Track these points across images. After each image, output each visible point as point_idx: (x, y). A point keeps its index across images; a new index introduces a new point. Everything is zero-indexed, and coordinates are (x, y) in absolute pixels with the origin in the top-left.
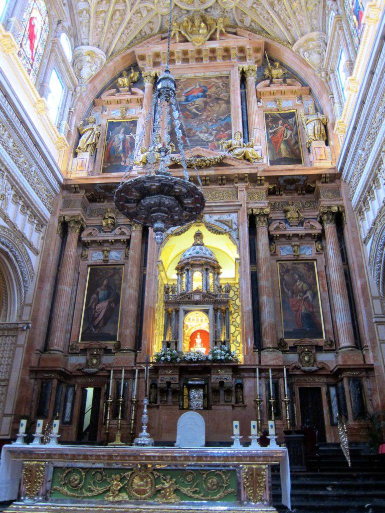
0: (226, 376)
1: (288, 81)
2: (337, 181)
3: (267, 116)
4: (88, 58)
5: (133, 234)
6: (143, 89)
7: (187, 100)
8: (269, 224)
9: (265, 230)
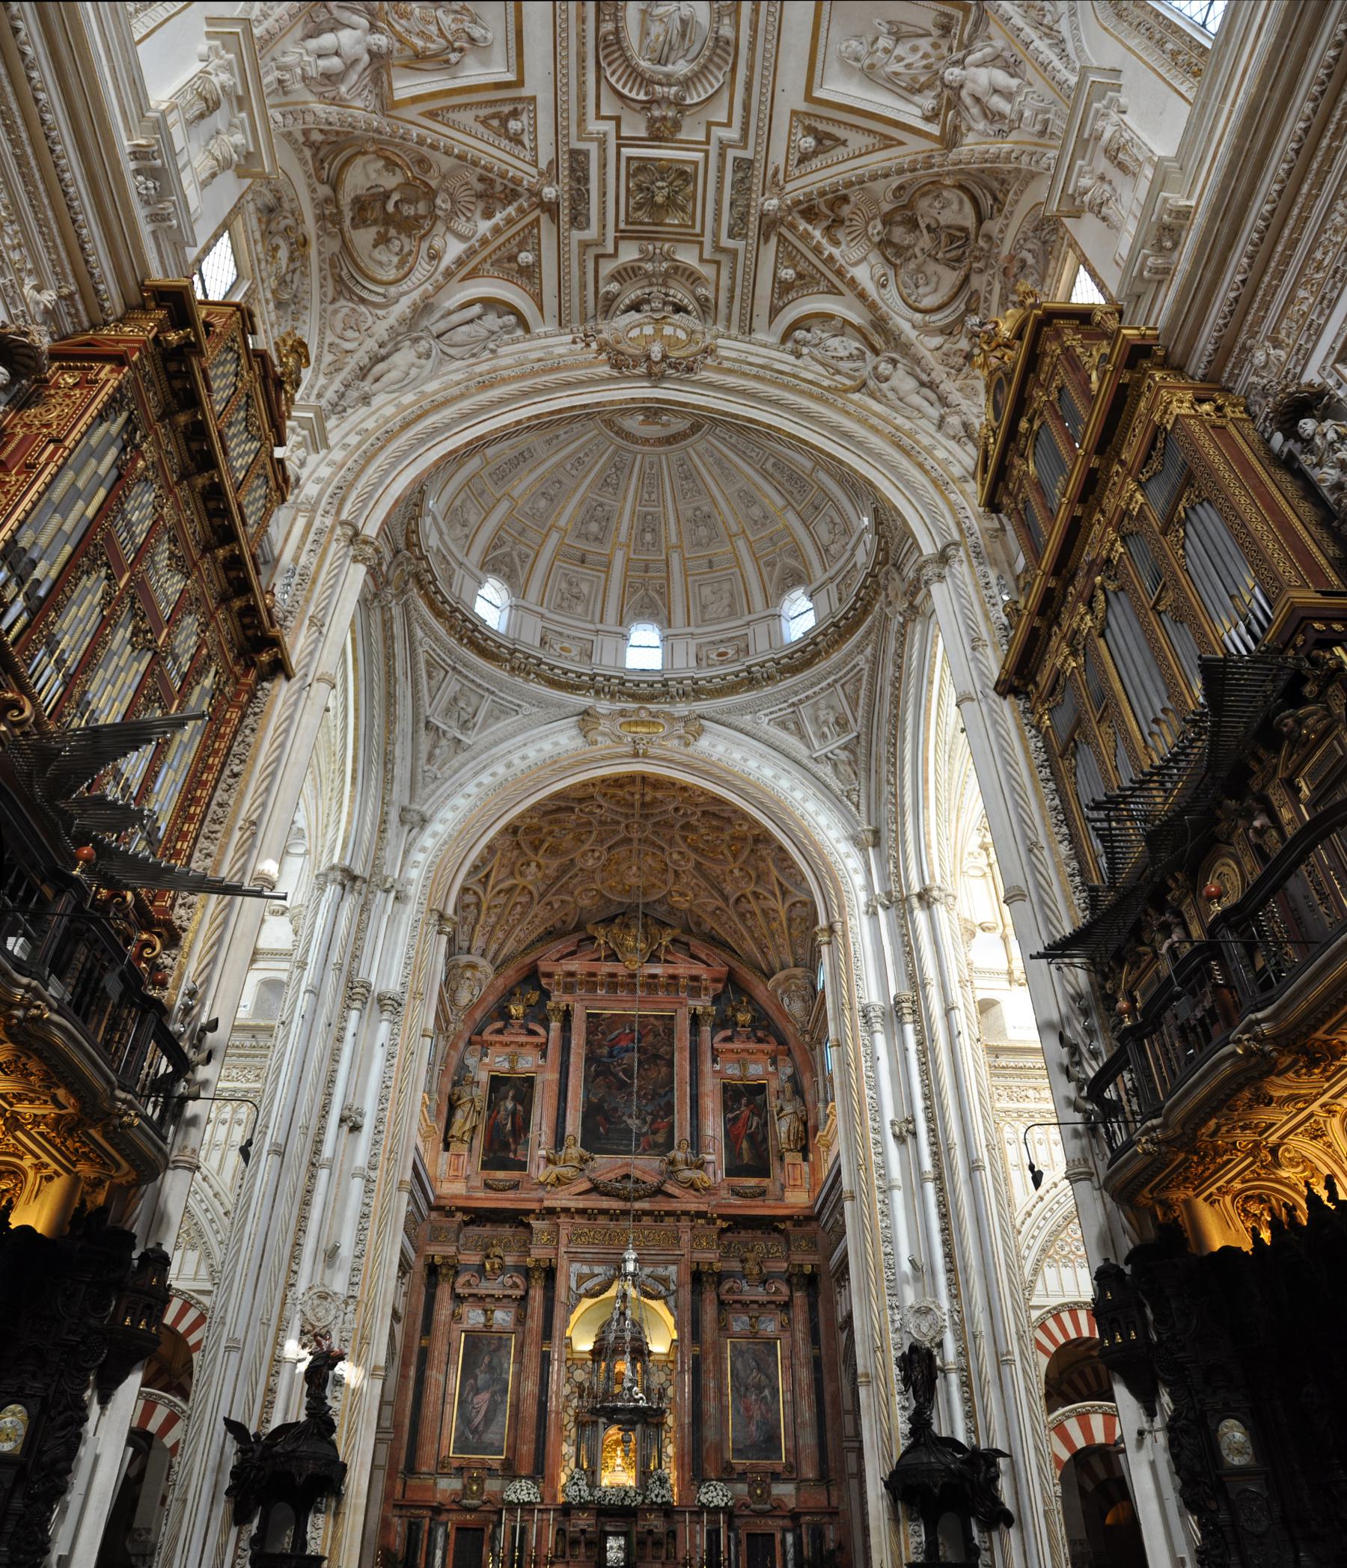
0: (656, 1522)
1: (760, 1034)
2: (814, 1224)
3: (725, 1087)
4: (468, 974)
5: (532, 1292)
6: (545, 1023)
7: (611, 1055)
8: (719, 1284)
9: (714, 1295)
